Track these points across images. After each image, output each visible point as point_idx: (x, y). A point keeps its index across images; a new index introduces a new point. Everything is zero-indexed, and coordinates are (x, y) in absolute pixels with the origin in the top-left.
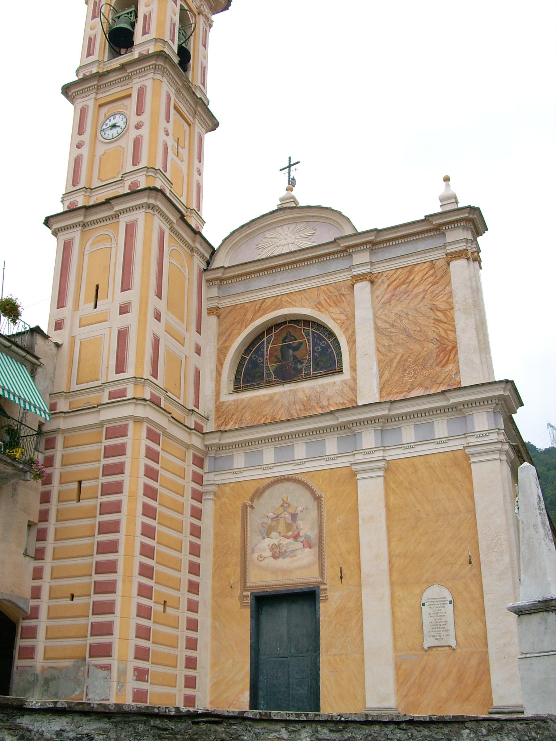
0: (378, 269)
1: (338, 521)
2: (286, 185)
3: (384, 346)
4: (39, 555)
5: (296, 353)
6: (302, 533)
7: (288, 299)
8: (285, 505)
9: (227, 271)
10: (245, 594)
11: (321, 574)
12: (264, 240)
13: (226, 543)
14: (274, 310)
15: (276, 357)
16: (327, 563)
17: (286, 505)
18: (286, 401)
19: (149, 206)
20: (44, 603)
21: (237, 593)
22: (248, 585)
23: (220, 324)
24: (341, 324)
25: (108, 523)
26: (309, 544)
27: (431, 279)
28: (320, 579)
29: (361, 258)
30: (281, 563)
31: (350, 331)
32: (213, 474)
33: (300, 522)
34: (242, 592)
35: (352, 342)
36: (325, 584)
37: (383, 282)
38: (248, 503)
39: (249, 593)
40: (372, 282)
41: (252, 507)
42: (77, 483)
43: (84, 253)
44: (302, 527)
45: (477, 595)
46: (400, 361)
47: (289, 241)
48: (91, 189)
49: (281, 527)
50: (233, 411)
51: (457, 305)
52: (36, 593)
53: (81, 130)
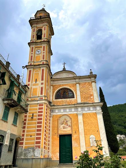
4: (24, 127)
8: (65, 119)
11: (72, 132)
16: (73, 130)
19: (46, 67)
20: (25, 137)
25: (39, 122)
33: (68, 122)
35: (76, 93)
52: (23, 135)
53: (32, 51)
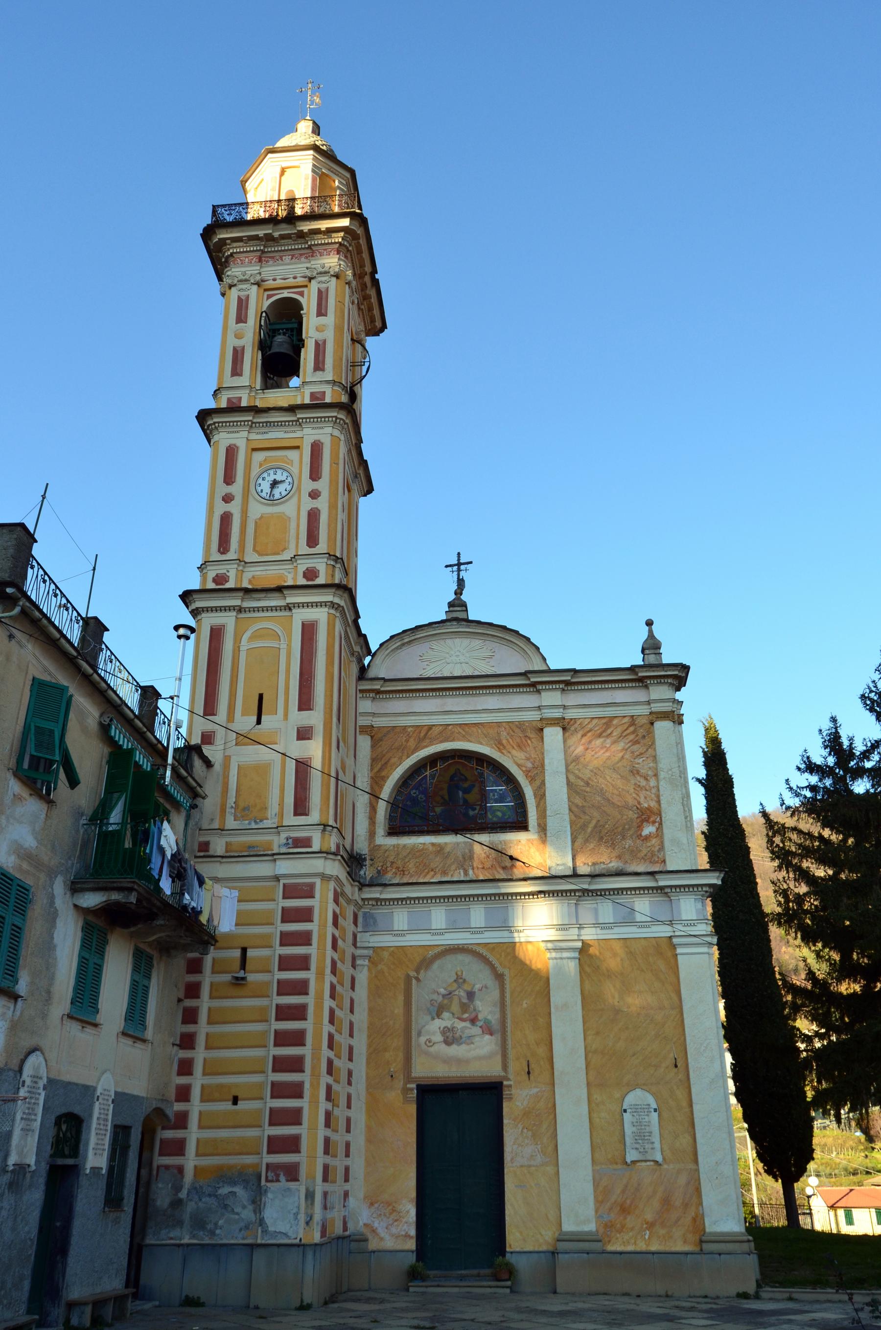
0: (570, 714)
1: (525, 1005)
2: (455, 587)
3: (577, 806)
4: (187, 1042)
5: (466, 796)
6: (480, 1017)
7: (461, 731)
8: (459, 980)
9: (388, 683)
10: (408, 1086)
11: (505, 1067)
12: (430, 652)
13: (384, 1021)
14: (441, 742)
15: (442, 798)
16: (511, 1054)
17: (461, 981)
18: (459, 854)
19: (333, 605)
20: (195, 1107)
21: (399, 1084)
22: (413, 1075)
23: (373, 746)
24: (527, 773)
25: (290, 1007)
26: (489, 1030)
27: (632, 737)
28: (503, 1074)
29: (551, 697)
30: (454, 1050)
31: (538, 783)
32: (368, 934)
33: (478, 1003)
34: (405, 1084)
35: (541, 796)
36: (508, 1079)
37: (576, 730)
38: (413, 974)
39: (414, 1086)
40: (564, 729)
41: (418, 979)
42: (239, 950)
43: (239, 647)
44: (480, 1009)
45: (684, 1104)
46: (595, 827)
47: (462, 658)
48: (246, 563)
49: (455, 1007)
50: (392, 858)
51: (662, 773)
52: (184, 1094)
53: (229, 479)
